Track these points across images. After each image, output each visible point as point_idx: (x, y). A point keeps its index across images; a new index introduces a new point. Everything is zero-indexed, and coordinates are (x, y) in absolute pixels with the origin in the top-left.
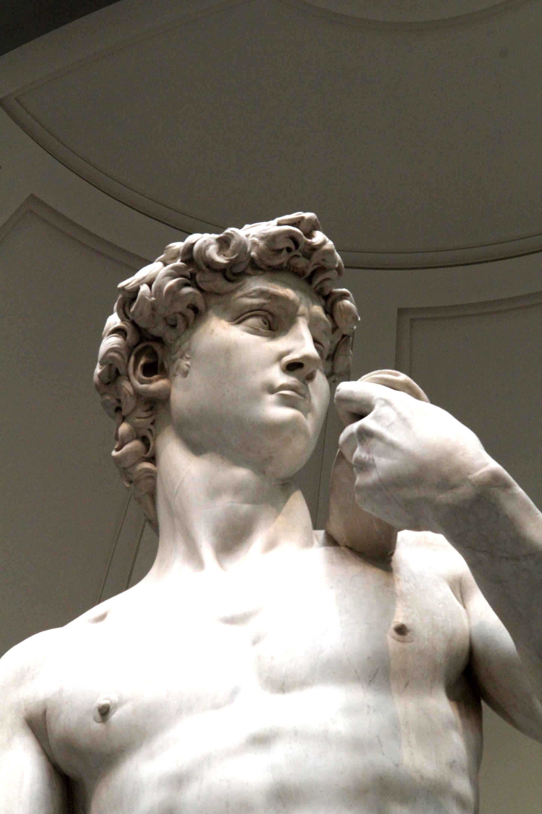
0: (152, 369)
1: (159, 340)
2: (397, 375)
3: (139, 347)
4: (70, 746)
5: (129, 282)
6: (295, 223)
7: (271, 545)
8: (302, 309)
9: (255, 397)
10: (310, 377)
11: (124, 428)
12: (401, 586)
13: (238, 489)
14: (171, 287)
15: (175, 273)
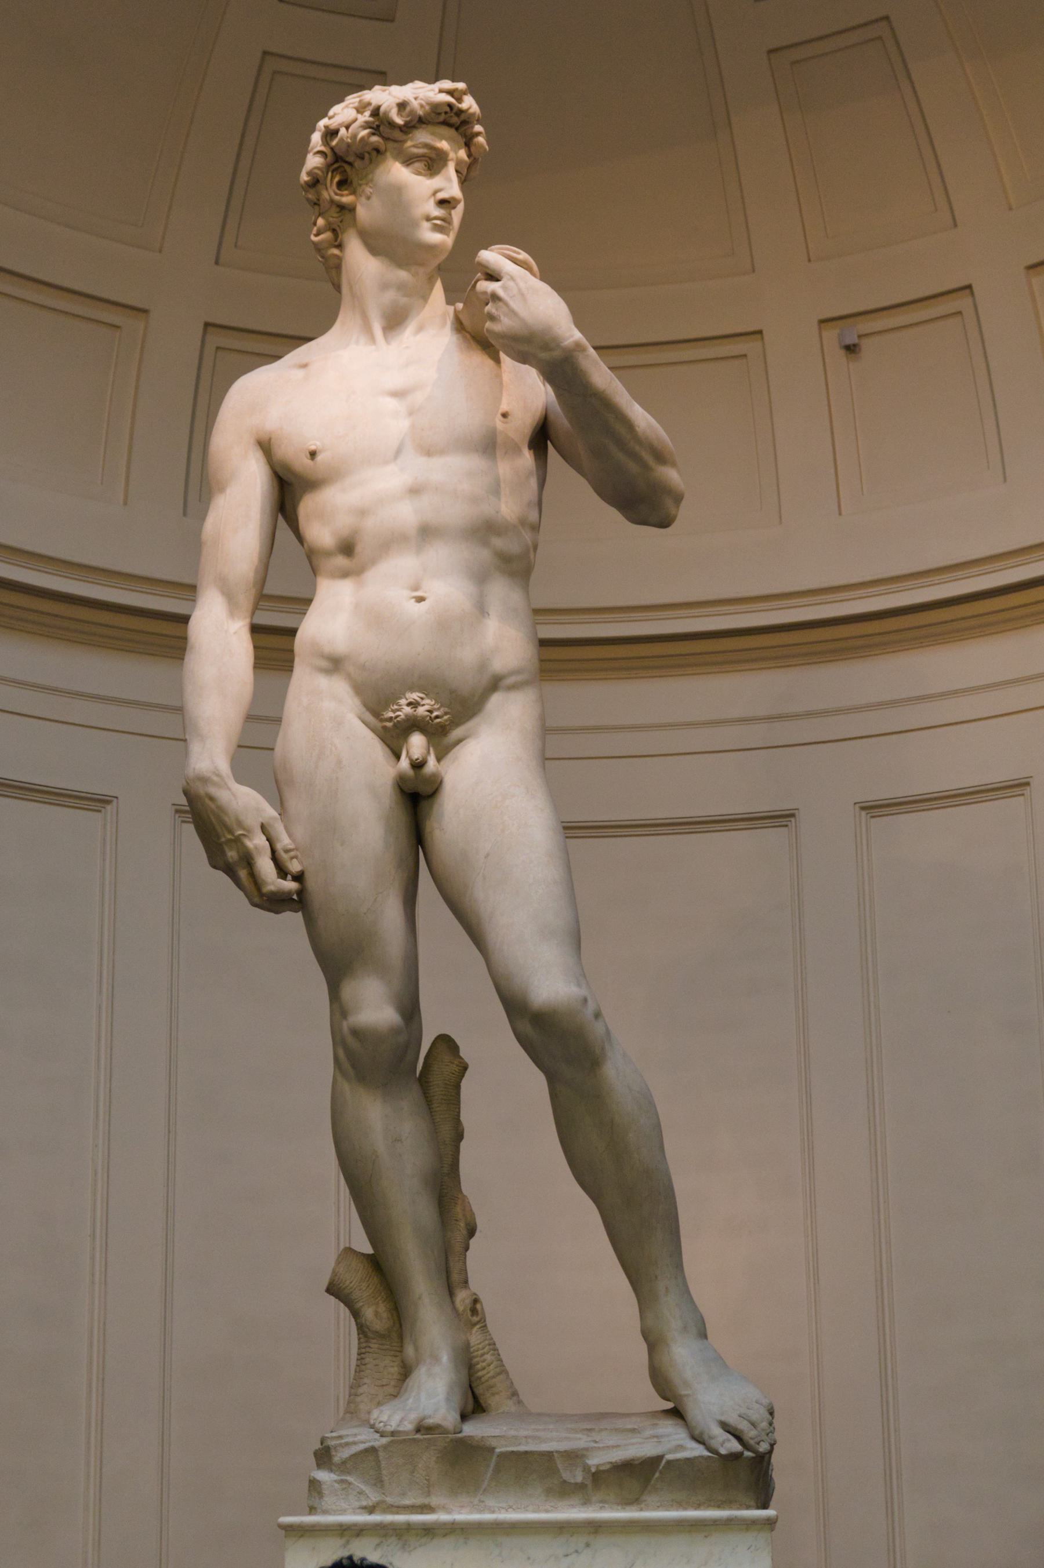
0: (343, 184)
1: (350, 164)
2: (519, 253)
3: (336, 166)
4: (287, 468)
7: (420, 329)
8: (452, 155)
9: (415, 224)
10: (454, 208)
11: (321, 222)
12: (506, 377)
13: (401, 287)
14: (362, 138)
15: (367, 125)
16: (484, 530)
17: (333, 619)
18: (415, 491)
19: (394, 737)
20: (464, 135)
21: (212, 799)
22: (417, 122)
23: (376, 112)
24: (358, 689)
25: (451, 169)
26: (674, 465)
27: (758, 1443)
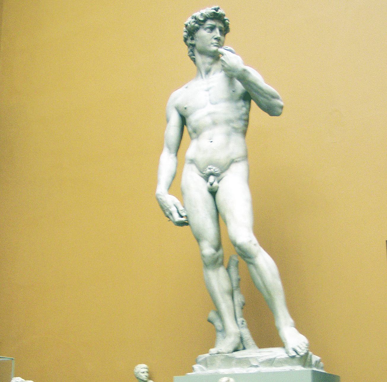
0: (192, 39)
5: (186, 23)
6: (215, 9)
9: (209, 46)
16: (228, 122)
17: (193, 150)
18: (209, 114)
19: (206, 178)
20: (221, 20)
21: (161, 199)
22: (206, 19)
23: (195, 18)
24: (198, 167)
25: (217, 30)
26: (278, 98)
27: (300, 353)
